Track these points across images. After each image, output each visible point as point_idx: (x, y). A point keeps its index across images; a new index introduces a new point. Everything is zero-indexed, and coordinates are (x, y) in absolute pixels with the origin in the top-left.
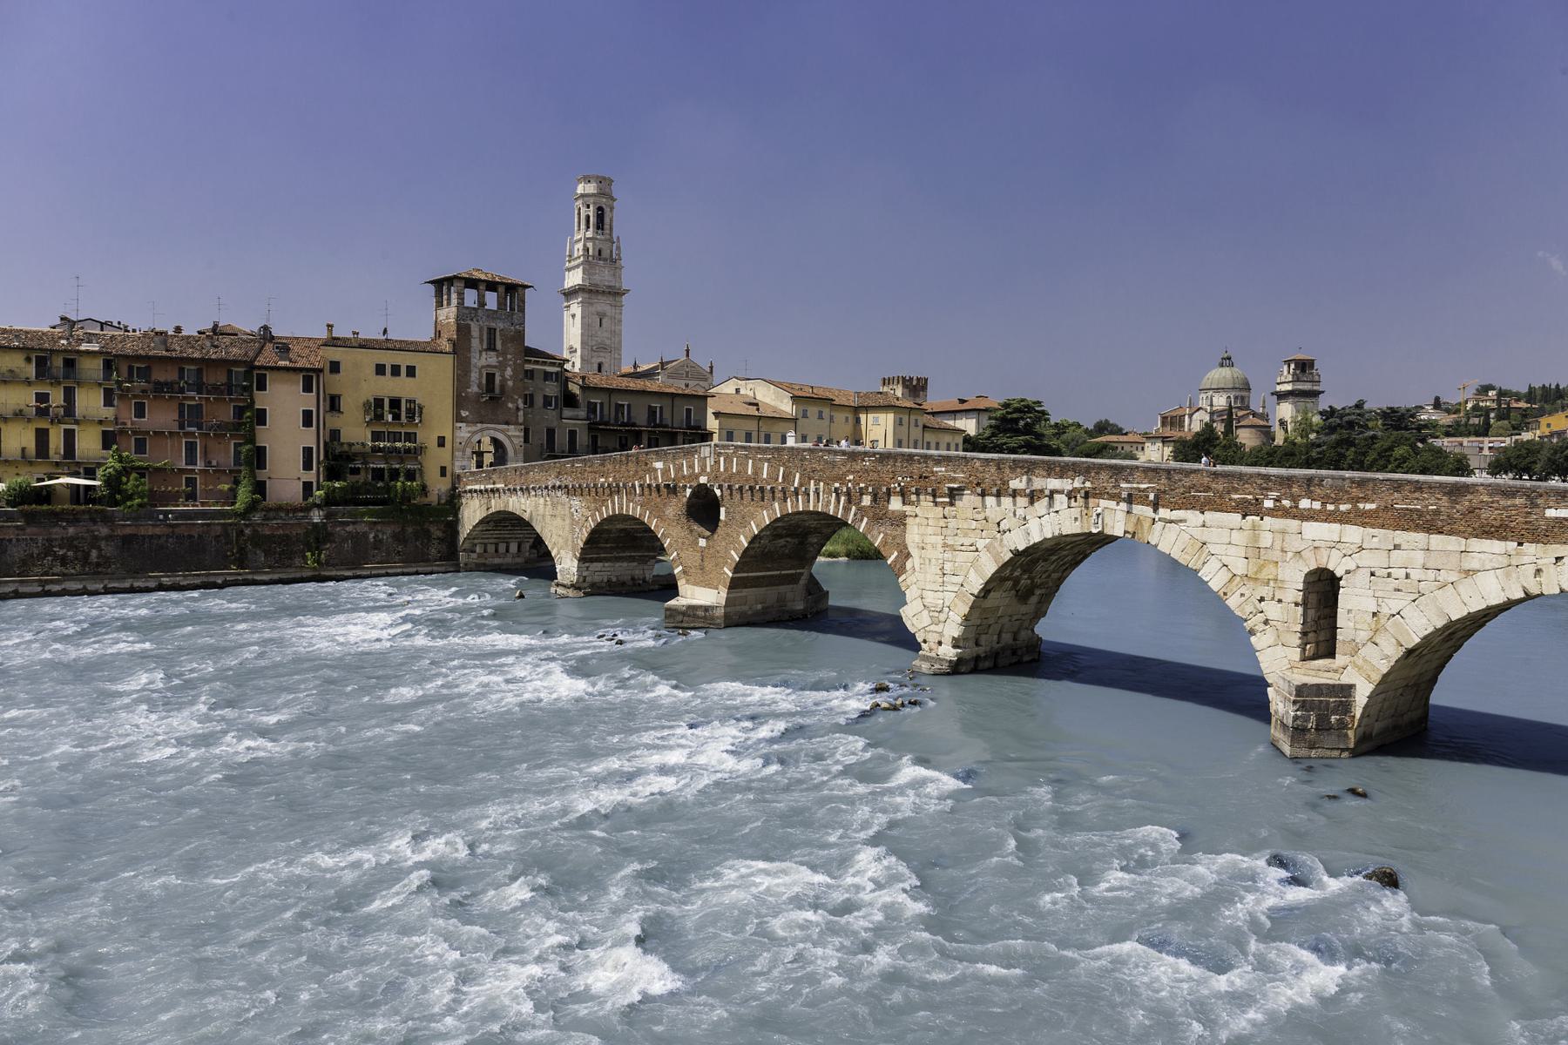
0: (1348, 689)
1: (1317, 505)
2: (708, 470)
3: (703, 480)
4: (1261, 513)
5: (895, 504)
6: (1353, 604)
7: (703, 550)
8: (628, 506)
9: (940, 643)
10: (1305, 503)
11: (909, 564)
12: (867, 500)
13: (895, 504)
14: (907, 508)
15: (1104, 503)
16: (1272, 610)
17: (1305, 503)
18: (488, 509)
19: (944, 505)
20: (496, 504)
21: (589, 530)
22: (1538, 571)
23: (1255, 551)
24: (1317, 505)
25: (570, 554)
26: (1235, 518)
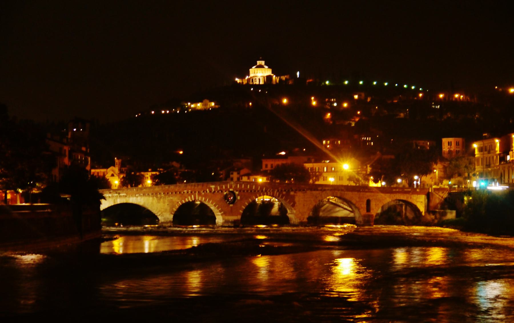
0: (372, 215)
1: (368, 190)
2: (233, 187)
3: (231, 190)
4: (361, 192)
5: (292, 193)
6: (373, 204)
7: (231, 207)
8: (198, 198)
9: (304, 219)
10: (366, 190)
11: (296, 205)
12: (284, 193)
13: (292, 193)
14: (295, 194)
15: (336, 191)
16: (363, 206)
17: (366, 190)
18: (114, 202)
19: (304, 193)
20: (119, 201)
21: (179, 205)
22: (393, 198)
23: (360, 198)
24: (368, 190)
25: (169, 213)
26: (356, 193)
